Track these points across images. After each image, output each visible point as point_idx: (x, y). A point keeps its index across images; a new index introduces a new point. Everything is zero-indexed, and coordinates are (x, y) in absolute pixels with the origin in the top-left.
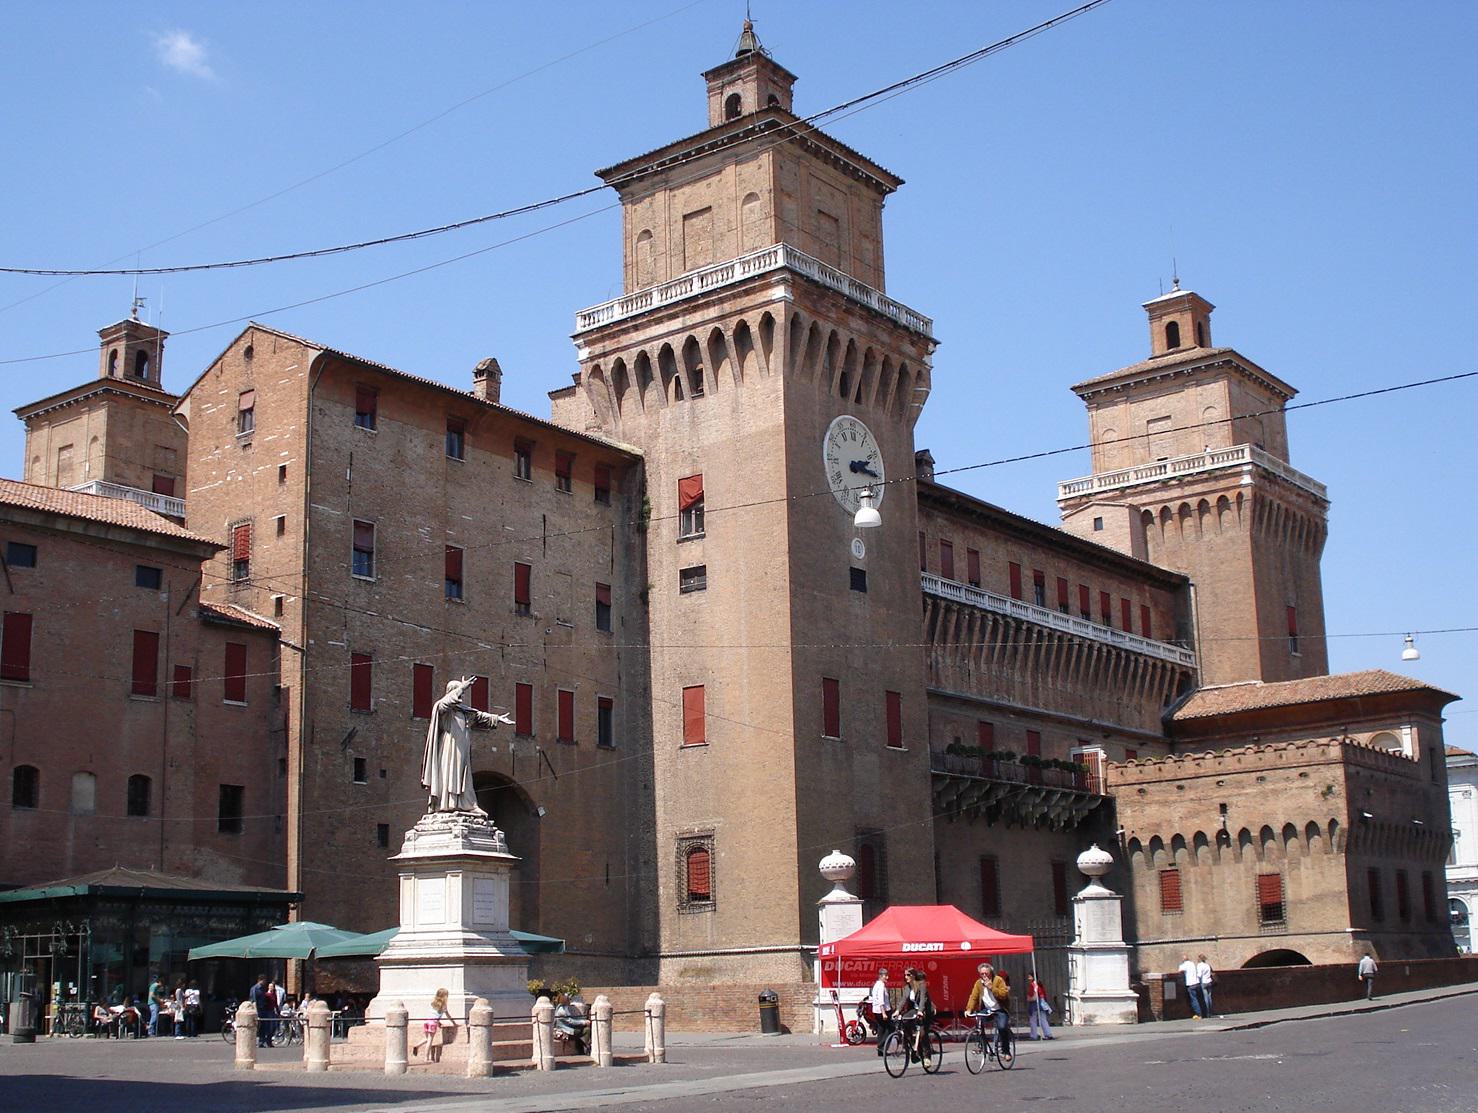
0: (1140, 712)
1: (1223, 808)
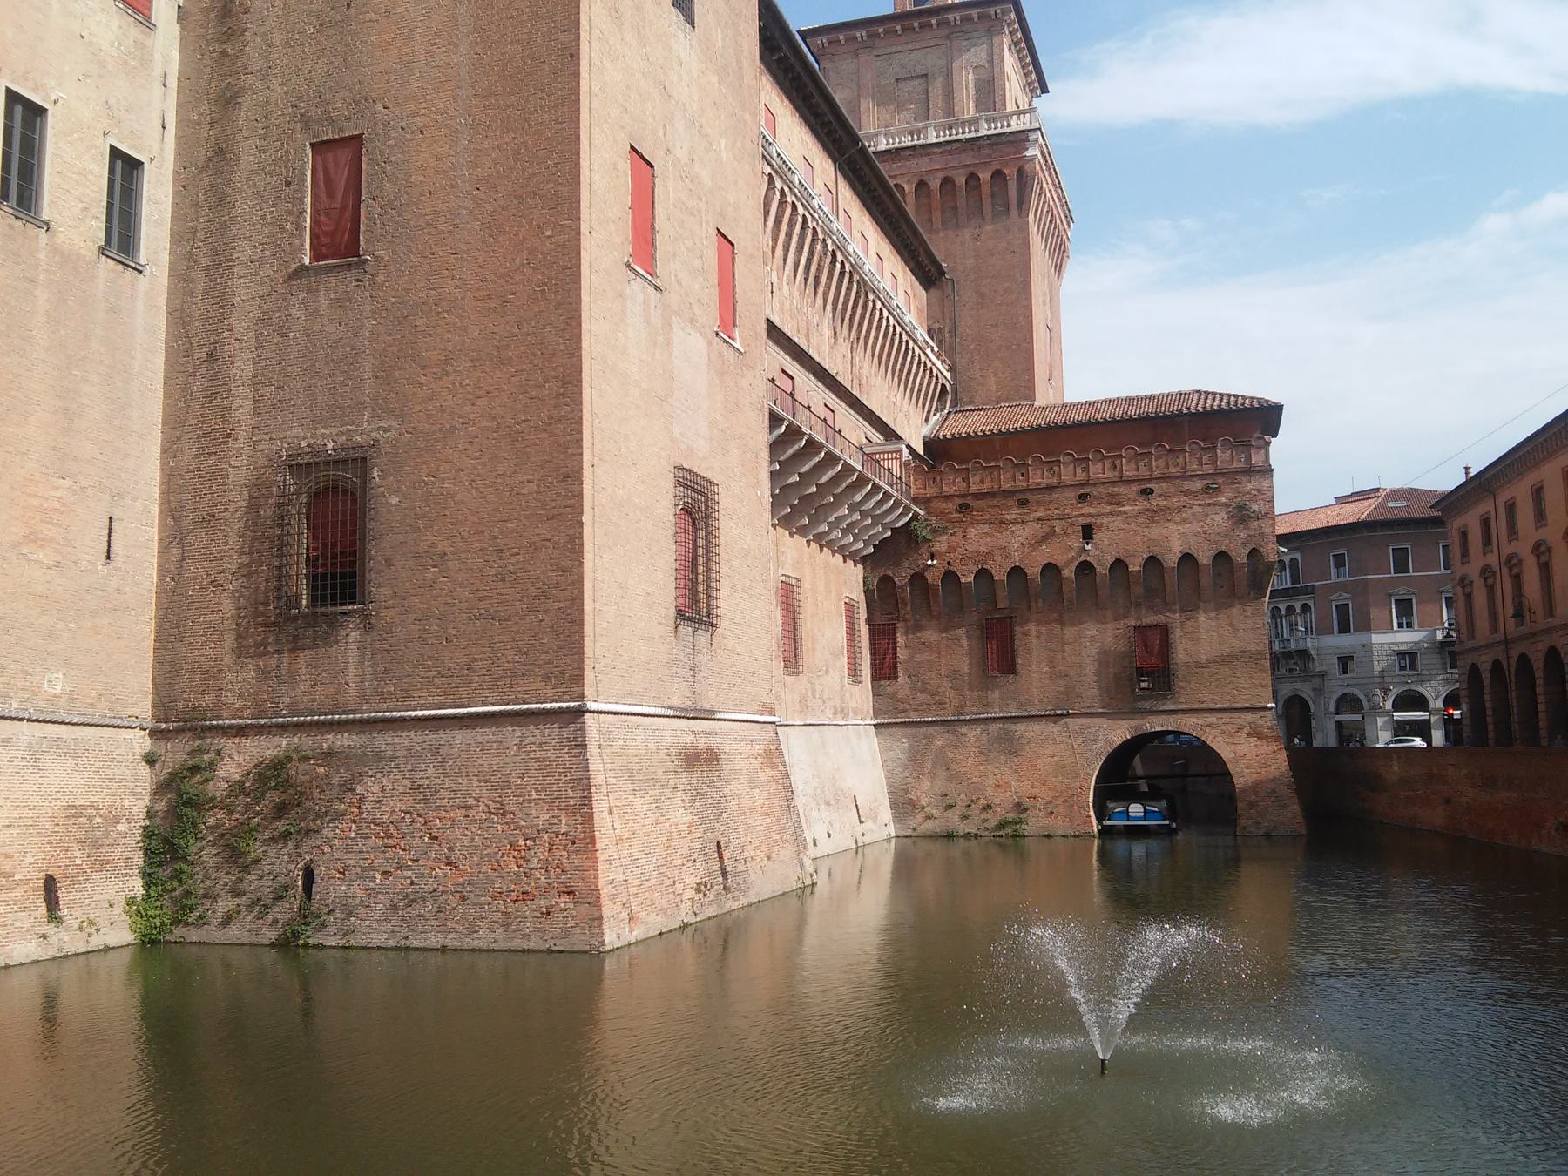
0: (909, 421)
1: (1088, 533)
